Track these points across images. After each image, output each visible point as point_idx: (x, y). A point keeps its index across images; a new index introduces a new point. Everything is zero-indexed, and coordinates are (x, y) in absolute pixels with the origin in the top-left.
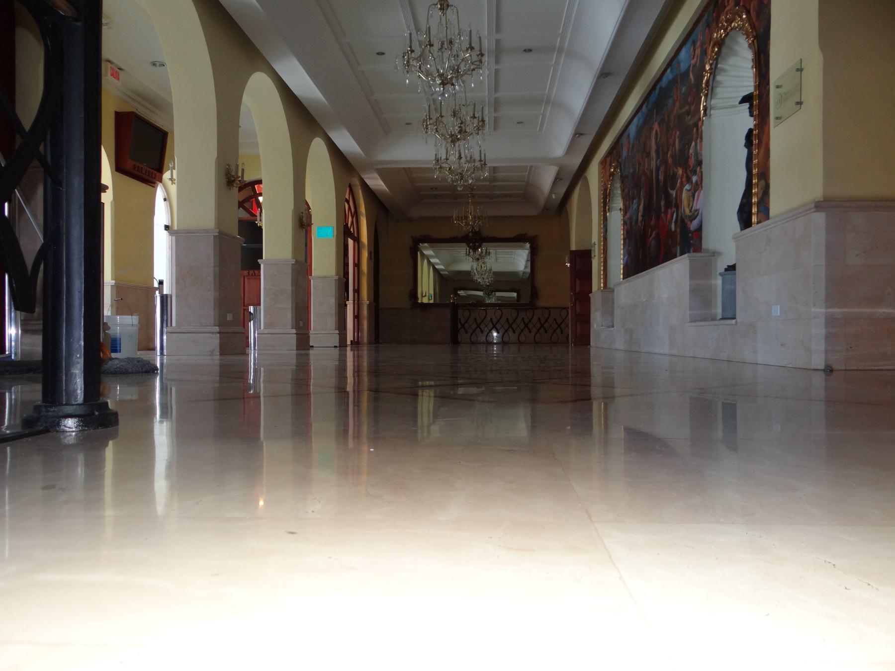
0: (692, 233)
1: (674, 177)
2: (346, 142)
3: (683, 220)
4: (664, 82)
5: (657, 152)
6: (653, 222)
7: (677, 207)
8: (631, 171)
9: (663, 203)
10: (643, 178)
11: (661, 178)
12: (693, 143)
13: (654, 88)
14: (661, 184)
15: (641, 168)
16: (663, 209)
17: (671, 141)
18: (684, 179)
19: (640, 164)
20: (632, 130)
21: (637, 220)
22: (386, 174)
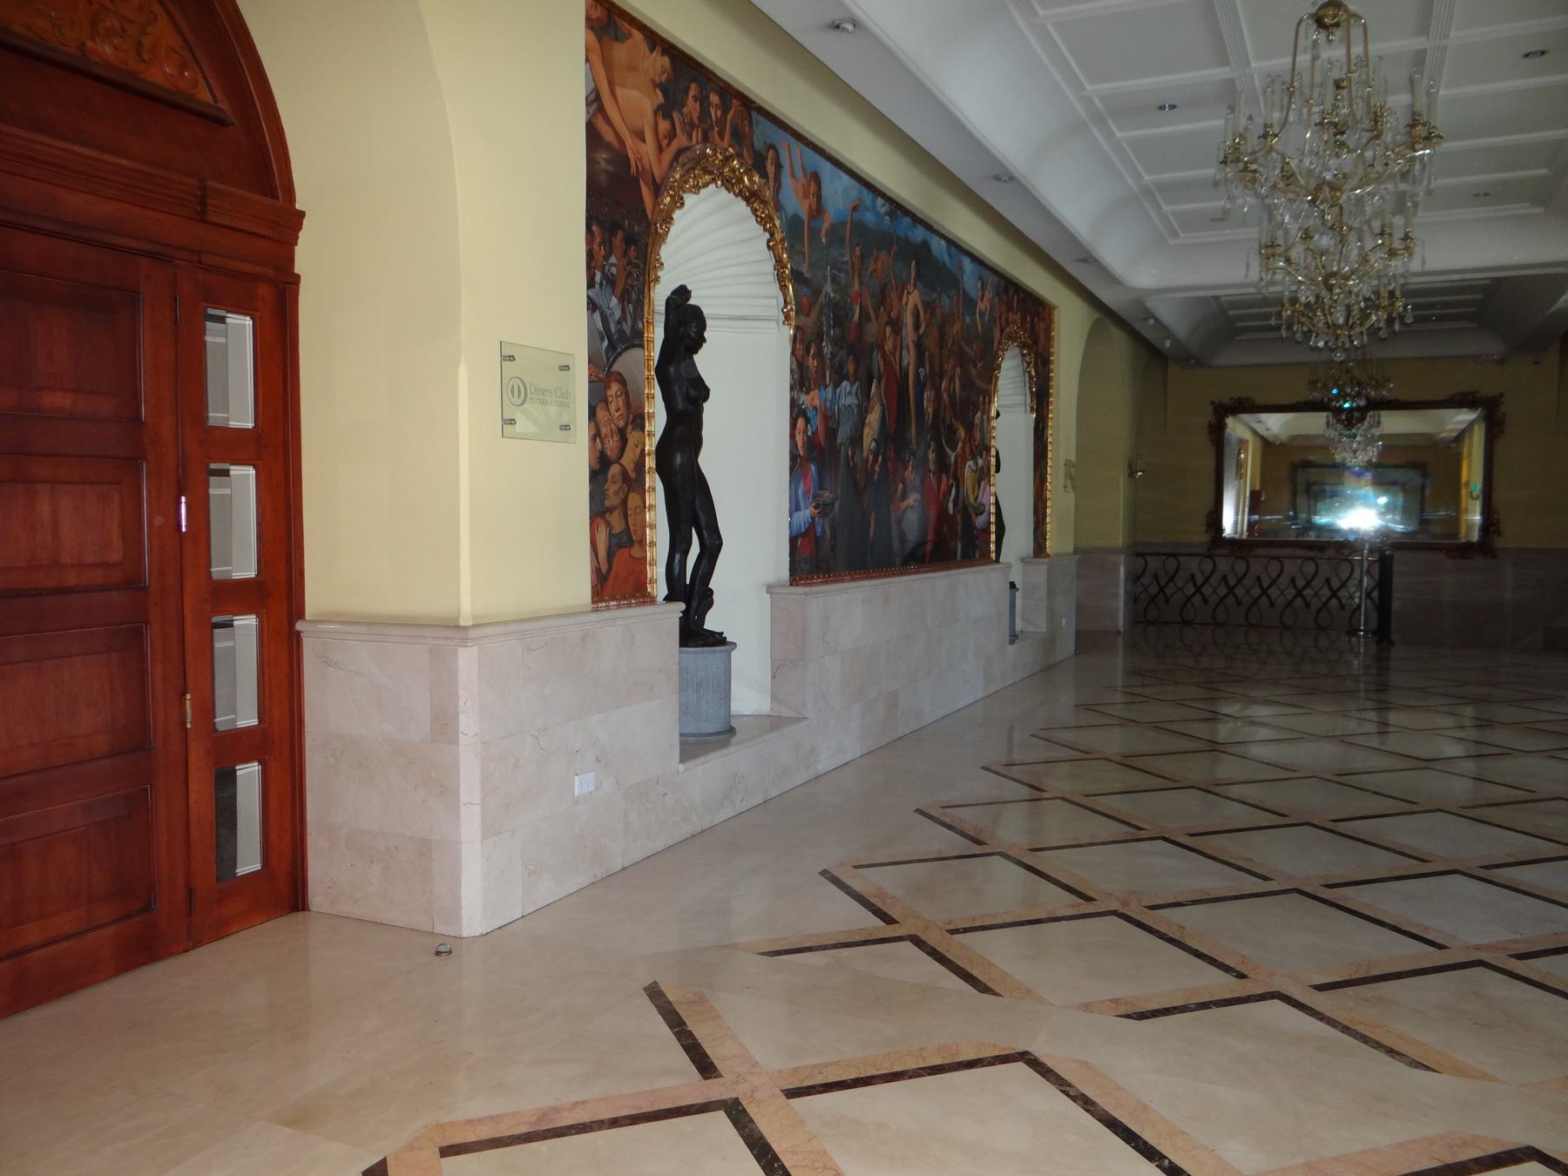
1: (952, 431)
3: (965, 508)
4: (938, 246)
7: (958, 480)
9: (932, 456)
11: (929, 409)
14: (929, 418)
15: (872, 329)
17: (948, 367)
21: (856, 440)
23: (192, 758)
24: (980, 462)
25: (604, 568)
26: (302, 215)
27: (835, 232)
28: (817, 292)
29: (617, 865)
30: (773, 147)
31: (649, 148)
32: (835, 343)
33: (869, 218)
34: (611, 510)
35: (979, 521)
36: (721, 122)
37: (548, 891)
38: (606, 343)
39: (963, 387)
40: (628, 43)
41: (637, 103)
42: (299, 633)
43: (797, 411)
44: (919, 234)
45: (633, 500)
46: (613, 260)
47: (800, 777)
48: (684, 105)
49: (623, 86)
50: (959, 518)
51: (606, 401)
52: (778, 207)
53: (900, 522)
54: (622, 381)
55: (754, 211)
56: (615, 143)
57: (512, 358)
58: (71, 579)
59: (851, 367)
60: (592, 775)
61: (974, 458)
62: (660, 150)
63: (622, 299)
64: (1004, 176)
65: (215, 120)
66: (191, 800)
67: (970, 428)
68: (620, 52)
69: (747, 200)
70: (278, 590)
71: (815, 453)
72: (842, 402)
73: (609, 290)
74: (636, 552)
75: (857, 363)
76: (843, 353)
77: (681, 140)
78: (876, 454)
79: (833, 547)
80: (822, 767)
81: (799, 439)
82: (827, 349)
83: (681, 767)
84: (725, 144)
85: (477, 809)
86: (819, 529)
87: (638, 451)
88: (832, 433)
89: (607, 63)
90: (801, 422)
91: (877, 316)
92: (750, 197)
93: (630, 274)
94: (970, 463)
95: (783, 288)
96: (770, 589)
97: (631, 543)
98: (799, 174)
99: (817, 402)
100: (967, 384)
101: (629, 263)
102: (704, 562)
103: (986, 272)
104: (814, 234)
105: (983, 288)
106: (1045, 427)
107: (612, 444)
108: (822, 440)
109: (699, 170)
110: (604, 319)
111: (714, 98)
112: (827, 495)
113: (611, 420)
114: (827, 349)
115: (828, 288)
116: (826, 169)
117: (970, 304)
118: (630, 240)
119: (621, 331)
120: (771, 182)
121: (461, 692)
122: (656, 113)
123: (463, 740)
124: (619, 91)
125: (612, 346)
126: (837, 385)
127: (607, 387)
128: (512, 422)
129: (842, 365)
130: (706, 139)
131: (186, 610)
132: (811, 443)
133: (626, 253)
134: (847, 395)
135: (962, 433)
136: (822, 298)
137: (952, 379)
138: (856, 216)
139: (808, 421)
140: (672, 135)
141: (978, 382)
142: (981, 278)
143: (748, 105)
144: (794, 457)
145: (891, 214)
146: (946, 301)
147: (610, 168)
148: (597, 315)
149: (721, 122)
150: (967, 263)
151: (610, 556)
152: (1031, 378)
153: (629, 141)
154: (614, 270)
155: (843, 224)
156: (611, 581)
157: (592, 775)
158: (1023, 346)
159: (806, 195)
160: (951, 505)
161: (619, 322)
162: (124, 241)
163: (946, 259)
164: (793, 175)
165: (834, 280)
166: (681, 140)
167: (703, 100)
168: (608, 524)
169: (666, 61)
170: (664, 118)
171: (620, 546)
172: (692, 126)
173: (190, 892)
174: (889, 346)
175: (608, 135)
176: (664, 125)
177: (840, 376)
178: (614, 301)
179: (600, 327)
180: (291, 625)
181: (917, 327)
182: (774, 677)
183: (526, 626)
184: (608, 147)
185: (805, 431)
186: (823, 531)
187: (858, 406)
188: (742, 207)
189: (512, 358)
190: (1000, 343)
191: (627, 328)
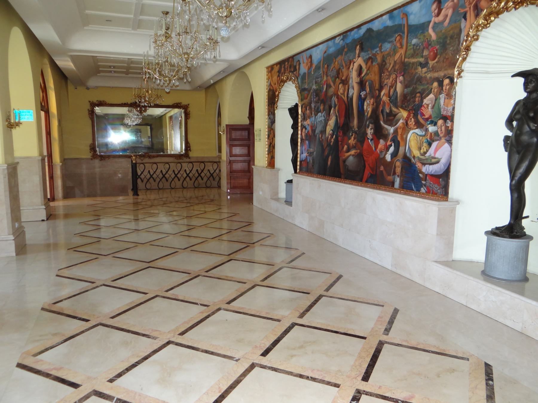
2: (45, 32)
4: (376, 26)
5: (362, 85)
6: (352, 141)
8: (314, 87)
9: (370, 132)
10: (334, 99)
12: (431, 96)
13: (359, 27)
15: (331, 91)
16: (370, 136)
17: (389, 82)
18: (412, 122)
19: (329, 86)
20: (317, 55)
21: (324, 131)
22: (74, 59)
27: (318, 68)
32: (316, 102)
39: (406, 86)
50: (398, 164)
53: (344, 161)
67: (416, 110)
68: (273, 72)
75: (324, 105)
76: (319, 104)
79: (313, 166)
81: (303, 135)
88: (314, 131)
90: (304, 130)
91: (334, 83)
94: (418, 131)
99: (309, 123)
107: (271, 141)
112: (311, 150)
114: (313, 105)
126: (316, 115)
129: (318, 108)
132: (307, 135)
134: (321, 117)
136: (312, 91)
137: (393, 85)
138: (325, 55)
139: (306, 129)
143: (292, 57)
160: (388, 158)
163: (389, 23)
175: (272, 88)
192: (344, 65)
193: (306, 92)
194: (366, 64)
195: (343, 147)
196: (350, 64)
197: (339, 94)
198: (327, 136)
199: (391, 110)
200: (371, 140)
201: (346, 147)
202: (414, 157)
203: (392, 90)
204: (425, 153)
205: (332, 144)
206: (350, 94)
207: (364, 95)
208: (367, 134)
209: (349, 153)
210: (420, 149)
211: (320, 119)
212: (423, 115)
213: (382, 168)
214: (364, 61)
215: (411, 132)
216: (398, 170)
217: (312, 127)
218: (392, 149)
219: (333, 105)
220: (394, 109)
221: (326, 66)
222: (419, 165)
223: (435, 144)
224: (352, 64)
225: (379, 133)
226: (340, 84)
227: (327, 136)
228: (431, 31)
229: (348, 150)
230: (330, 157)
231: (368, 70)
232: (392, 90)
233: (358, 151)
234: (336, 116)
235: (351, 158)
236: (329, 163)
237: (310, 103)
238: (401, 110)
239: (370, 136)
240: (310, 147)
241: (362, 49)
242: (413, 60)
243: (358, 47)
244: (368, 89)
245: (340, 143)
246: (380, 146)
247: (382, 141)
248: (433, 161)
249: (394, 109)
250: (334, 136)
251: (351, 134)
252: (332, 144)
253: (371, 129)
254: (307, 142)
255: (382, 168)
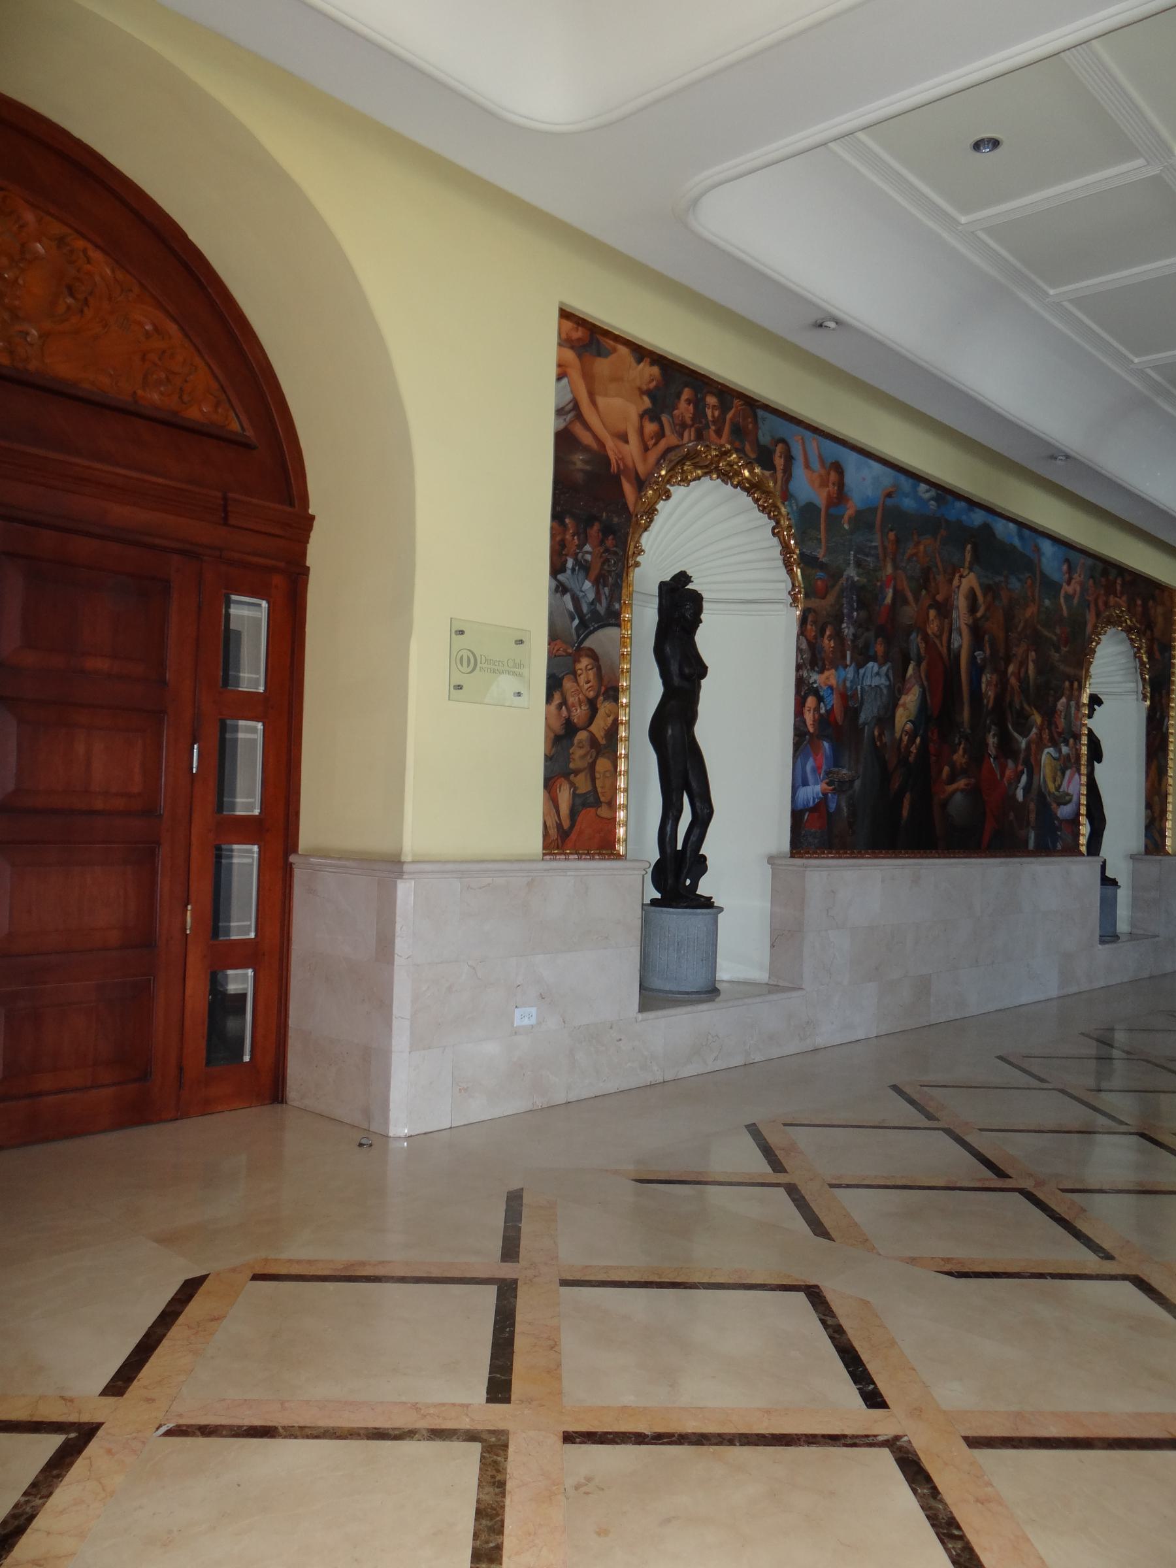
0: (1061, 821)
5: (977, 632)
6: (959, 757)
7: (1032, 767)
9: (992, 740)
12: (1064, 700)
15: (909, 613)
16: (992, 750)
17: (1019, 651)
18: (1046, 736)
21: (886, 719)
23: (191, 959)
24: (1065, 750)
25: (566, 824)
26: (312, 518)
27: (863, 520)
28: (836, 575)
29: (560, 1098)
30: (783, 441)
31: (633, 448)
32: (858, 624)
33: (908, 504)
34: (576, 772)
35: (1064, 811)
36: (719, 423)
37: (478, 1110)
38: (576, 621)
39: (1039, 672)
40: (613, 357)
41: (619, 410)
42: (291, 864)
43: (803, 690)
44: (978, 518)
45: (602, 764)
46: (588, 548)
47: (792, 1048)
48: (675, 407)
49: (606, 395)
50: (1032, 806)
51: (574, 673)
52: (786, 496)
53: (944, 805)
54: (593, 655)
55: (756, 501)
56: (594, 445)
57: (462, 632)
58: (99, 805)
59: (879, 648)
60: (533, 1010)
61: (1055, 744)
62: (646, 449)
63: (596, 583)
64: (1055, 454)
65: (245, 445)
66: (188, 992)
67: (1050, 715)
68: (602, 366)
69: (748, 491)
70: (278, 826)
71: (824, 729)
72: (867, 682)
73: (581, 575)
74: (603, 812)
76: (871, 634)
77: (671, 439)
78: (913, 736)
80: (820, 1041)
81: (809, 717)
82: (848, 630)
83: (640, 1016)
84: (723, 441)
85: (407, 1023)
86: (832, 806)
87: (610, 720)
88: (852, 713)
89: (588, 377)
90: (811, 701)
91: (917, 600)
92: (751, 488)
93: (608, 560)
94: (1051, 750)
95: (790, 571)
96: (771, 860)
97: (598, 803)
98: (816, 464)
99: (833, 682)
100: (1044, 668)
101: (607, 550)
102: (696, 831)
103: (1073, 555)
104: (834, 521)
105: (1070, 570)
106: (1165, 716)
107: (579, 714)
108: (839, 718)
109: (686, 465)
110: (576, 600)
111: (711, 400)
113: (579, 690)
114: (848, 630)
115: (851, 572)
116: (851, 461)
117: (1052, 587)
118: (608, 530)
119: (594, 612)
120: (780, 475)
121: (398, 919)
122: (642, 417)
123: (398, 961)
124: (600, 400)
125: (583, 624)
126: (860, 665)
127: (577, 660)
128: (459, 687)
129: (867, 646)
130: (700, 437)
131: (193, 839)
132: (825, 722)
133: (602, 542)
134: (875, 675)
135: (1037, 718)
136: (843, 581)
137: (1023, 663)
138: (889, 502)
139: (820, 699)
140: (661, 434)
141: (1062, 667)
142: (1067, 561)
143: (752, 404)
144: (800, 734)
145: (937, 499)
146: (1015, 584)
147: (588, 468)
148: (567, 598)
149: (719, 423)
150: (1047, 547)
151: (573, 814)
152: (1142, 664)
153: (610, 444)
154: (588, 557)
155: (873, 510)
156: (573, 836)
157: (533, 1010)
158: (1128, 630)
159: (824, 483)
161: (592, 603)
162: (158, 541)
163: (1017, 542)
164: (807, 466)
165: (859, 564)
166: (671, 439)
167: (698, 404)
168: (572, 785)
169: (655, 370)
170: (652, 420)
171: (585, 805)
172: (684, 426)
173: (181, 1069)
174: (933, 627)
175: (586, 438)
176: (650, 428)
177: (863, 656)
178: (588, 585)
179: (571, 607)
180: (286, 856)
181: (973, 608)
182: (772, 946)
183: (464, 867)
184: (586, 449)
185: (817, 709)
186: (838, 807)
187: (889, 687)
188: (745, 500)
189: (462, 632)
190: (1095, 627)
191: (601, 609)
192: (940, 564)
193: (820, 574)
194: (985, 596)
195: (940, 771)
196: (954, 575)
197: (930, 632)
198: (897, 735)
199: (1022, 708)
200: (995, 759)
201: (946, 769)
202: (1049, 793)
203: (1023, 670)
204: (1060, 786)
205: (911, 759)
206: (956, 645)
207: (983, 660)
208: (987, 745)
209: (954, 786)
210: (1054, 781)
211: (876, 681)
212: (1057, 727)
213: (1012, 816)
214: (981, 585)
215: (1046, 750)
216: (1032, 817)
217: (844, 697)
218: (1024, 779)
219: (913, 654)
220: (1026, 706)
221: (892, 535)
222: (1054, 805)
223: (1068, 773)
224: (957, 575)
225: (1007, 748)
226: (930, 606)
227: (897, 735)
228: (1062, 600)
229: (952, 779)
230: (908, 796)
231: (987, 609)
232: (1023, 670)
233: (973, 780)
234: (922, 686)
235: (958, 797)
236: (905, 813)
237: (838, 619)
238: (1035, 712)
239: (992, 750)
240: (837, 763)
241: (976, 558)
242: (1046, 633)
243: (969, 547)
244: (988, 652)
245: (933, 758)
246: (1008, 772)
247: (1010, 764)
248: (1067, 798)
249: (1026, 706)
250: (918, 740)
251: (957, 741)
252: (911, 759)
253: (994, 735)
254: (826, 745)
255: (1012, 816)
